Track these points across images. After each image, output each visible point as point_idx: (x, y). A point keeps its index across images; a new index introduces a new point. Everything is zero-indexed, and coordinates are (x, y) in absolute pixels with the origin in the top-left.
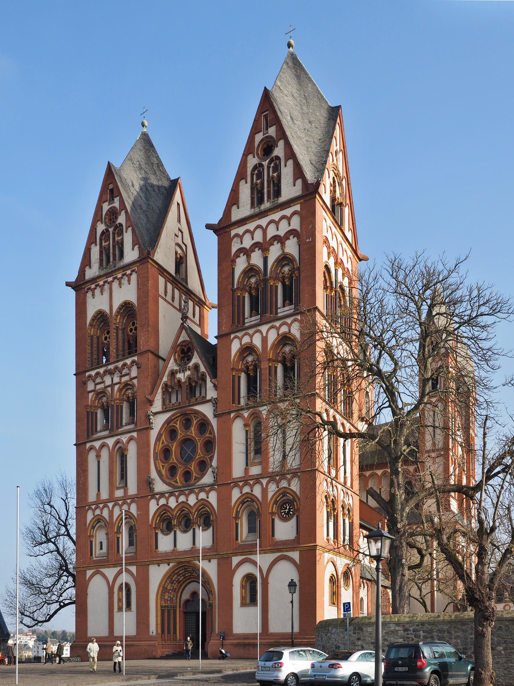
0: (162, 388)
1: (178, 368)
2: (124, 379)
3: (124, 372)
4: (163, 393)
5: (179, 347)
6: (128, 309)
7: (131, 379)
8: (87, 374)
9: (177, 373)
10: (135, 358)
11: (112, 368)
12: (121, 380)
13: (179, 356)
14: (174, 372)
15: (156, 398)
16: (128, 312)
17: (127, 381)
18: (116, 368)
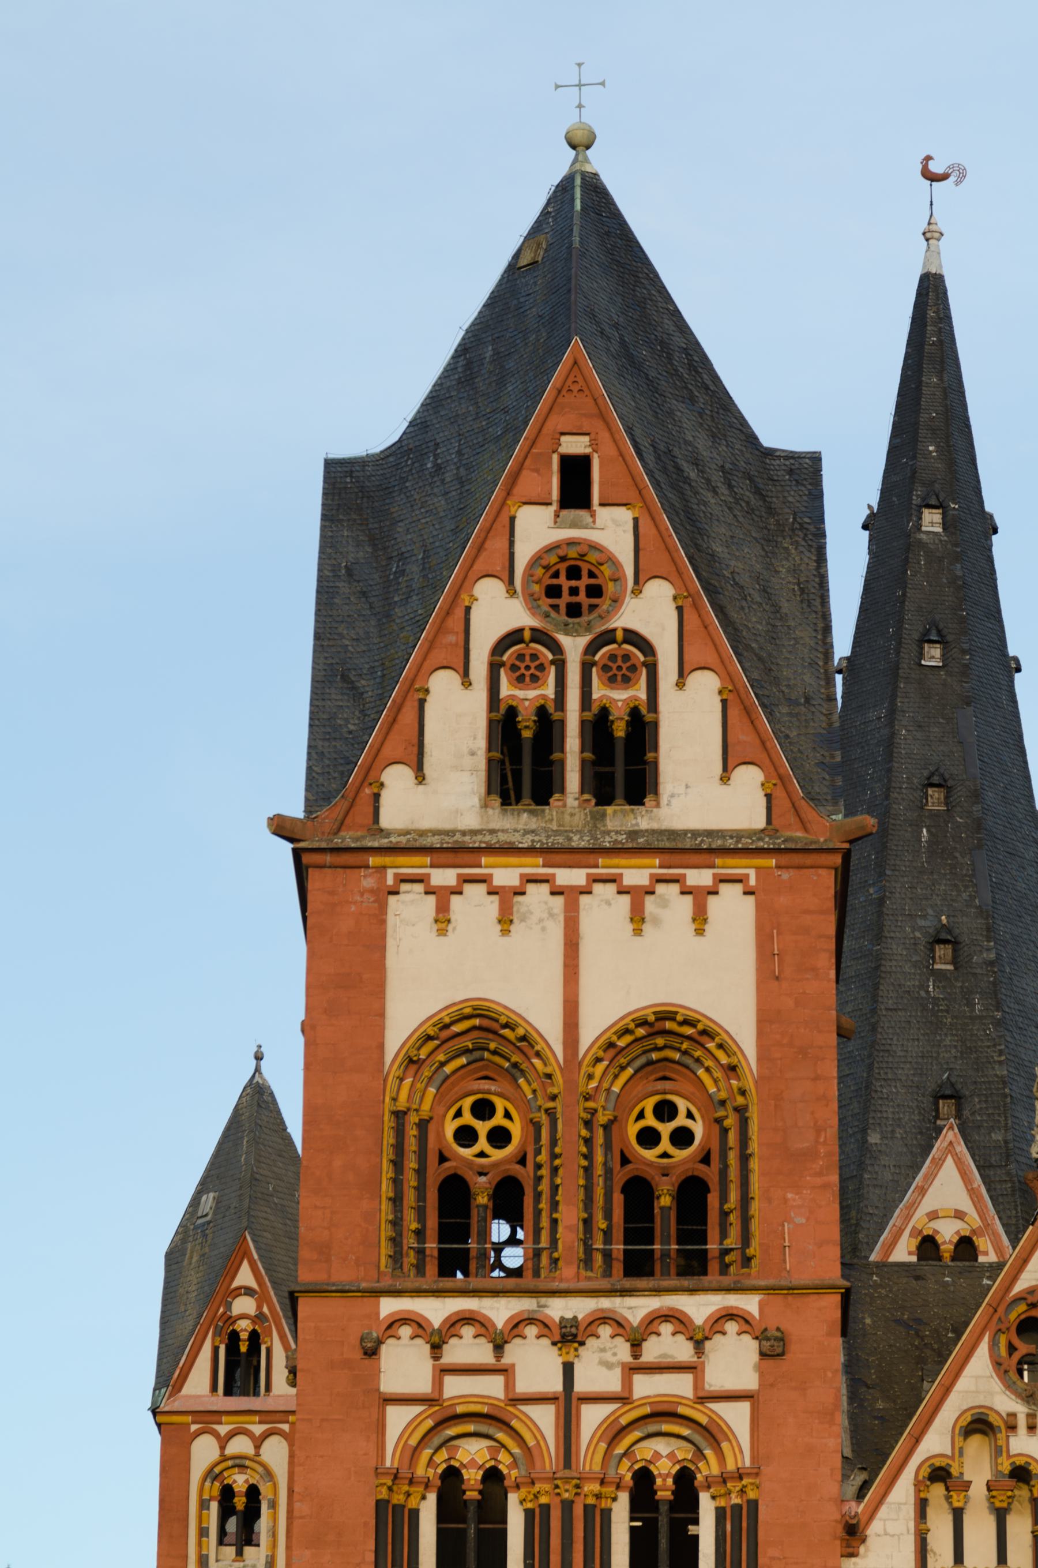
0: (917, 1484)
1: (1021, 1409)
2: (645, 1386)
3: (653, 1350)
4: (922, 1507)
5: (1022, 1307)
6: (660, 1041)
7: (703, 1398)
8: (388, 1306)
9: (1012, 1428)
10: (750, 1304)
11: (580, 1317)
12: (627, 1384)
13: (1012, 1349)
14: (993, 1419)
15: (875, 1528)
16: (645, 1052)
17: (680, 1400)
18: (604, 1318)
